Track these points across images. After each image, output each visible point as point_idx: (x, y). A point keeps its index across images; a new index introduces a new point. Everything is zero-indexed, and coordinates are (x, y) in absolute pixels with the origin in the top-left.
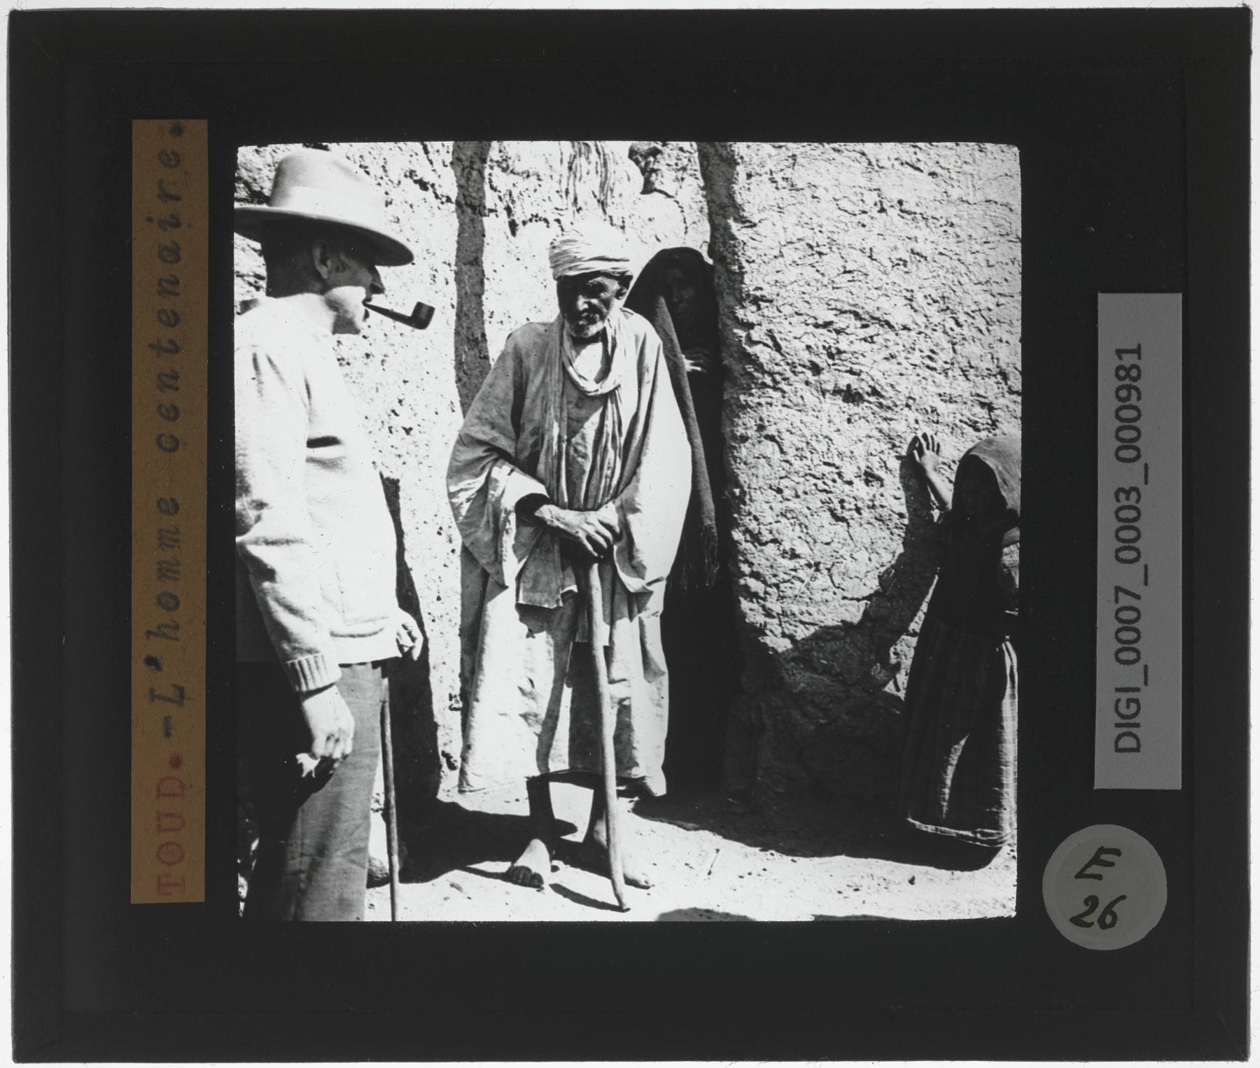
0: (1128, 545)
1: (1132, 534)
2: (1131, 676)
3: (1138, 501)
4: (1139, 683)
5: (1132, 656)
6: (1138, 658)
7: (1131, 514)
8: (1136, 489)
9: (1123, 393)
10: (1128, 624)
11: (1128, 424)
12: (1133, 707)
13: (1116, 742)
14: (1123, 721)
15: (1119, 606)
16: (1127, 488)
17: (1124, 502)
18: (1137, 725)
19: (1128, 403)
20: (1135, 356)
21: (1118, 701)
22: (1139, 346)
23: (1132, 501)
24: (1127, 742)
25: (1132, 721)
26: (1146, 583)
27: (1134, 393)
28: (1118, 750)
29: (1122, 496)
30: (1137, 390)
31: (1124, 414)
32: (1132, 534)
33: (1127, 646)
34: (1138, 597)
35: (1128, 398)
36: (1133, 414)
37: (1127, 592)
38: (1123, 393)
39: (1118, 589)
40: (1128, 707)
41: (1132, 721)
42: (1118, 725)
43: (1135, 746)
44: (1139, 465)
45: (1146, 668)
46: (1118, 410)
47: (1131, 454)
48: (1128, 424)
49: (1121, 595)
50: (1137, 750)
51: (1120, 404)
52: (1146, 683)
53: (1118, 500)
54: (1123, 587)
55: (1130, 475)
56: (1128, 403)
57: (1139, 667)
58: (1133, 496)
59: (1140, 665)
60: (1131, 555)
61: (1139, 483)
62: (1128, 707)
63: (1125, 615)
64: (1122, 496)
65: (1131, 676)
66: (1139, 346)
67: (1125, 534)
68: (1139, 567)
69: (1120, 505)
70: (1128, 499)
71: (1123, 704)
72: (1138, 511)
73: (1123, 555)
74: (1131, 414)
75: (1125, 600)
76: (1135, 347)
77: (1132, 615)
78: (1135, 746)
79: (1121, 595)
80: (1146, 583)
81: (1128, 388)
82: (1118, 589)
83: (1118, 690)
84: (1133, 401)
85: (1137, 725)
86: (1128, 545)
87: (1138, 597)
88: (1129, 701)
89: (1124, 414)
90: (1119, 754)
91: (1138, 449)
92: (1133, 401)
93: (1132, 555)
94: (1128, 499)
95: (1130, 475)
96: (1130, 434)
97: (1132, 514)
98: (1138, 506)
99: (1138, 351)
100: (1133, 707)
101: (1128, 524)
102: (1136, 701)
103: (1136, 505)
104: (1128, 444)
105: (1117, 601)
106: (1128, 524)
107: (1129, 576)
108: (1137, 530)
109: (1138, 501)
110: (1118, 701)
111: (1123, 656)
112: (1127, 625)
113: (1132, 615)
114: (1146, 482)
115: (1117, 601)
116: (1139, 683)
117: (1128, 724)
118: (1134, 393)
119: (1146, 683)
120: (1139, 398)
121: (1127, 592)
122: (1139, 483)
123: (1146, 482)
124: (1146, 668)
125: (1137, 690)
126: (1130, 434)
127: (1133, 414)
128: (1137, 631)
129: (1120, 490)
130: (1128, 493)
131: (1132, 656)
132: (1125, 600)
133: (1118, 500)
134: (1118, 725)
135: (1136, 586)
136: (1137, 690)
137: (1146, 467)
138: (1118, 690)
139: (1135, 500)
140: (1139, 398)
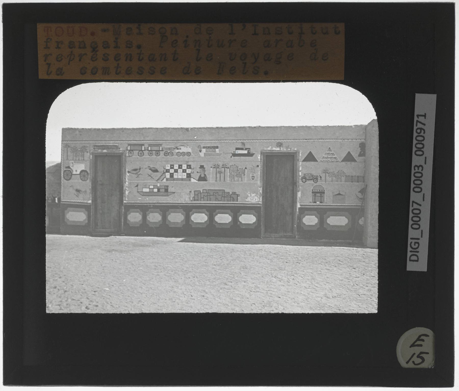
3: (422, 170)
4: (419, 237)
5: (417, 227)
6: (419, 228)
7: (419, 175)
8: (422, 166)
9: (419, 131)
12: (417, 245)
14: (413, 250)
16: (418, 165)
17: (417, 170)
18: (418, 252)
19: (421, 134)
20: (424, 117)
21: (411, 243)
22: (425, 114)
24: (414, 258)
25: (417, 250)
26: (424, 200)
27: (423, 131)
28: (410, 260)
29: (416, 168)
30: (424, 130)
33: (416, 223)
34: (420, 205)
35: (421, 132)
36: (422, 138)
38: (419, 131)
40: (415, 245)
41: (417, 250)
42: (411, 251)
45: (422, 231)
47: (420, 153)
48: (420, 142)
49: (414, 204)
50: (417, 261)
52: (422, 237)
53: (415, 170)
54: (415, 201)
56: (421, 134)
57: (419, 232)
58: (420, 168)
60: (419, 190)
61: (423, 164)
62: (415, 245)
63: (415, 211)
66: (425, 114)
70: (418, 169)
75: (415, 206)
76: (424, 114)
77: (418, 212)
79: (414, 204)
80: (424, 200)
81: (421, 129)
82: (413, 202)
83: (411, 239)
84: (422, 134)
85: (418, 252)
87: (420, 205)
88: (415, 243)
89: (418, 138)
90: (412, 262)
91: (423, 151)
92: (422, 134)
93: (419, 190)
94: (418, 169)
97: (420, 175)
98: (422, 172)
99: (425, 116)
100: (417, 245)
102: (418, 243)
103: (421, 172)
104: (419, 149)
105: (412, 206)
108: (421, 181)
109: (422, 170)
110: (411, 243)
112: (417, 215)
113: (418, 212)
114: (425, 163)
116: (419, 237)
117: (415, 251)
118: (423, 131)
119: (422, 237)
120: (424, 133)
123: (425, 163)
124: (422, 231)
127: (422, 138)
128: (420, 218)
129: (416, 166)
130: (418, 167)
131: (417, 226)
132: (415, 206)
133: (415, 170)
134: (411, 251)
136: (418, 239)
137: (426, 158)
138: (411, 239)
139: (421, 170)
140: (424, 133)
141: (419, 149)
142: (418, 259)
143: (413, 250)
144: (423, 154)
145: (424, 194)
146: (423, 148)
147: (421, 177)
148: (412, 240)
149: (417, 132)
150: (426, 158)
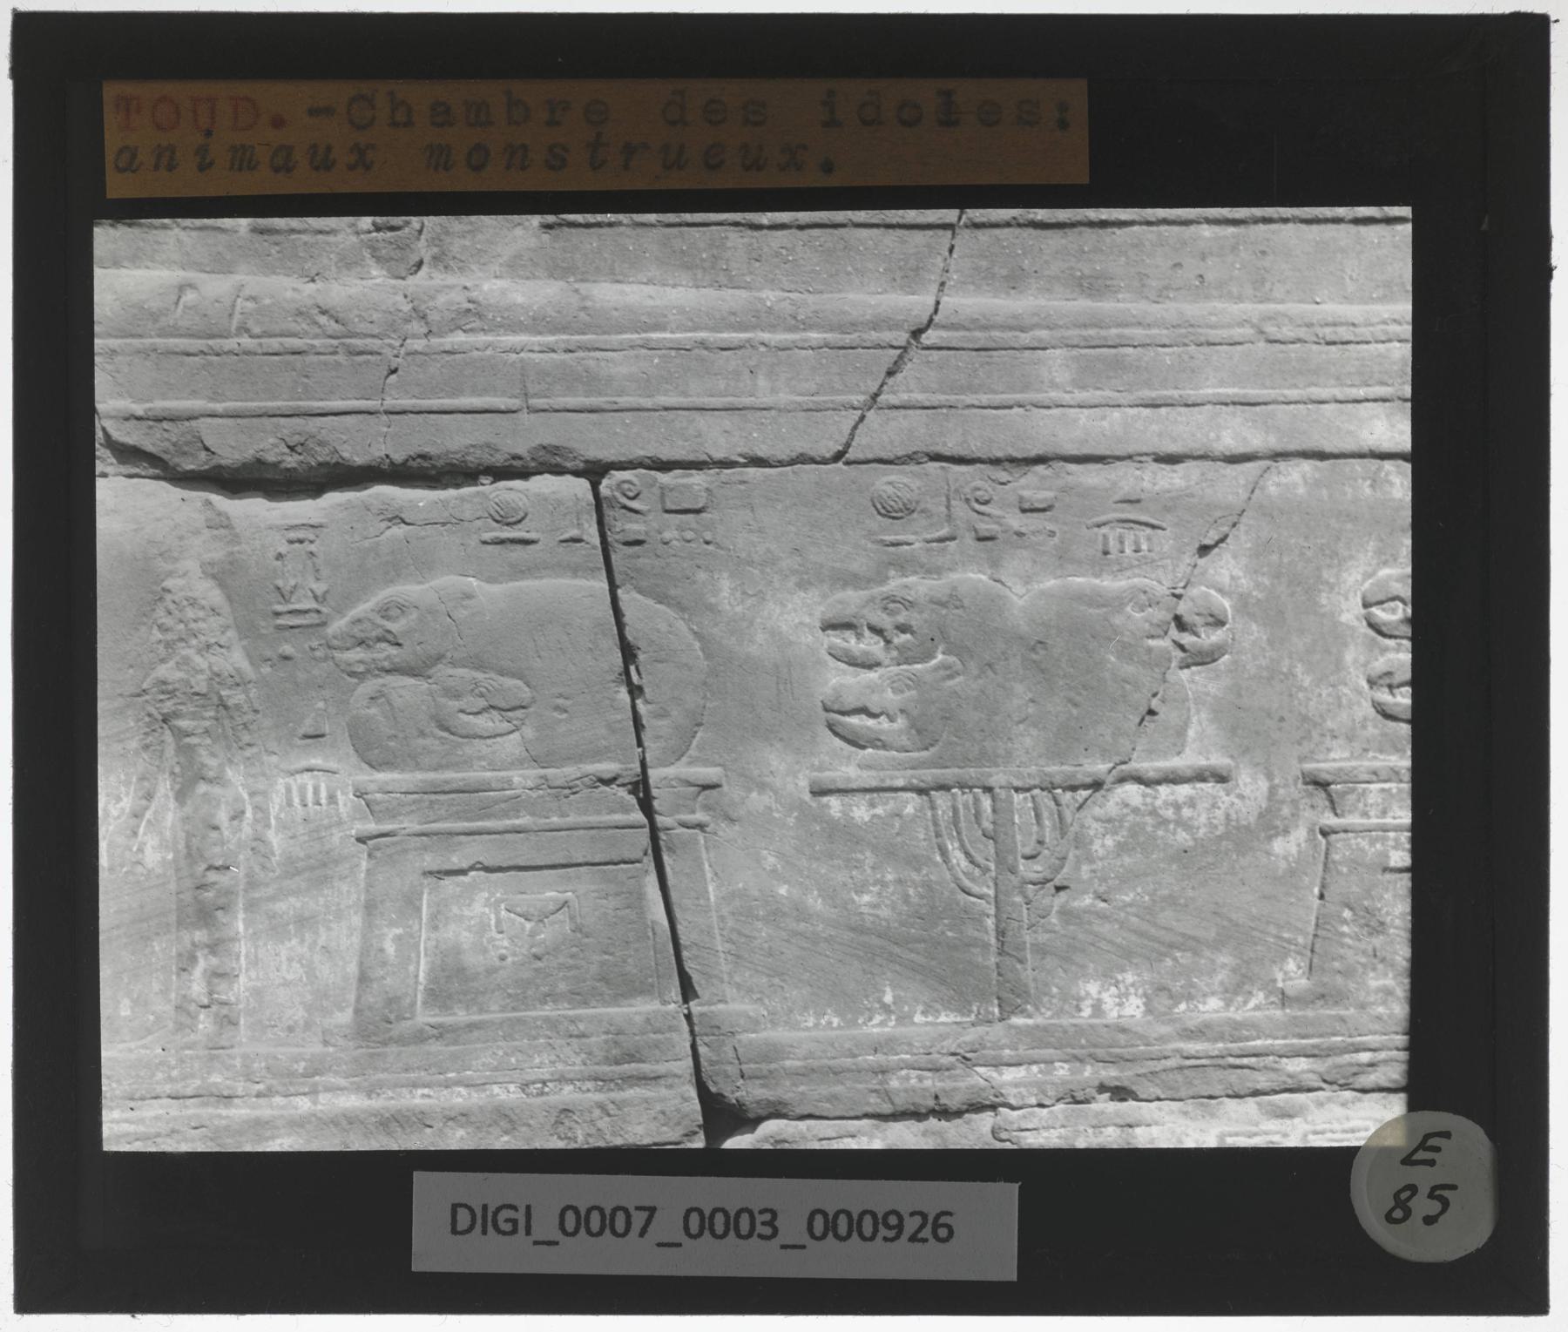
0: (707, 1223)
1: (719, 1229)
2: (546, 1226)
3: (761, 1236)
4: (538, 1233)
9: (893, 1220)
10: (610, 1222)
11: (855, 1226)
12: (507, 1227)
13: (461, 1205)
14: (490, 1215)
15: (632, 1211)
16: (777, 1223)
17: (760, 1219)
18: (484, 1232)
19: (880, 1226)
21: (514, 1208)
23: (760, 1229)
24: (464, 1218)
25: (490, 1229)
26: (659, 1245)
27: (891, 1234)
28: (455, 1207)
29: (767, 1217)
31: (868, 1221)
32: (719, 1229)
34: (643, 1233)
36: (868, 1228)
37: (648, 1221)
38: (893, 1220)
39: (652, 1210)
40: (507, 1221)
41: (490, 1229)
42: (485, 1208)
43: (459, 1228)
44: (805, 1239)
46: (874, 1215)
48: (855, 1226)
49: (645, 1215)
50: (454, 1231)
51: (880, 1216)
52: (536, 1243)
53: (761, 1212)
54: (655, 1221)
55: (792, 1227)
57: (556, 1235)
58: (767, 1231)
59: (558, 1236)
60: (694, 1228)
61: (783, 1238)
62: (507, 1221)
64: (767, 1217)
65: (546, 1226)
67: (719, 1219)
68: (680, 1236)
69: (757, 1215)
70: (763, 1223)
71: (505, 1214)
72: (750, 1235)
73: (694, 1218)
74: (868, 1228)
75: (639, 1219)
77: (620, 1225)
78: (459, 1228)
79: (645, 1215)
80: (659, 1245)
81: (900, 1227)
82: (652, 1210)
83: (528, 1208)
84: (883, 1232)
85: (484, 1232)
86: (707, 1223)
87: (643, 1233)
88: (514, 1222)
89: (868, 1221)
91: (824, 1236)
92: (883, 1232)
93: (694, 1228)
94: (763, 1223)
95: (792, 1227)
96: (843, 1228)
101: (732, 1224)
102: (514, 1231)
104: (831, 1226)
105: (638, 1208)
106: (732, 1224)
107: (668, 1225)
109: (761, 1236)
110: (514, 1208)
111: (570, 1219)
112: (608, 1223)
114: (784, 1247)
115: (638, 1208)
116: (538, 1233)
117: (487, 1220)
118: (891, 1234)
119: (536, 1243)
120: (886, 1239)
121: (648, 1221)
122: (783, 1238)
123: (784, 1247)
125: (528, 1233)
126: (843, 1228)
129: (774, 1214)
132: (639, 1219)
133: (761, 1212)
134: (485, 1208)
135: (657, 1232)
136: (528, 1233)
137: (803, 1247)
138: (528, 1208)
140: (886, 1239)
141: (831, 1226)
142: (461, 1233)
143: (490, 1215)
144: (812, 1236)
145: (680, 1245)
146: (837, 1236)
147: (739, 1236)
148: (522, 1210)
149: (887, 1214)
150: (803, 1247)
